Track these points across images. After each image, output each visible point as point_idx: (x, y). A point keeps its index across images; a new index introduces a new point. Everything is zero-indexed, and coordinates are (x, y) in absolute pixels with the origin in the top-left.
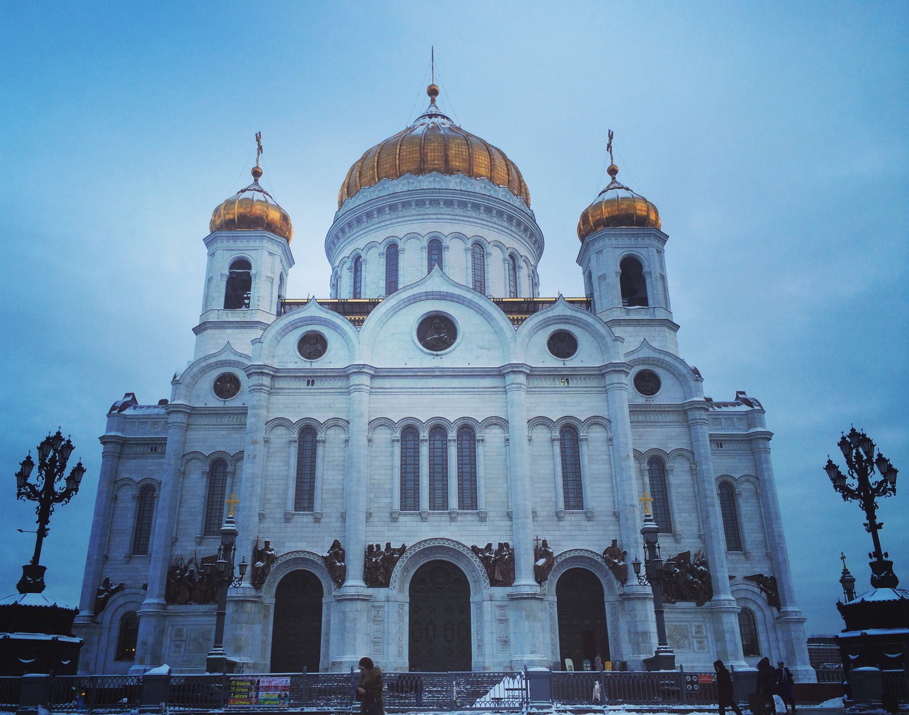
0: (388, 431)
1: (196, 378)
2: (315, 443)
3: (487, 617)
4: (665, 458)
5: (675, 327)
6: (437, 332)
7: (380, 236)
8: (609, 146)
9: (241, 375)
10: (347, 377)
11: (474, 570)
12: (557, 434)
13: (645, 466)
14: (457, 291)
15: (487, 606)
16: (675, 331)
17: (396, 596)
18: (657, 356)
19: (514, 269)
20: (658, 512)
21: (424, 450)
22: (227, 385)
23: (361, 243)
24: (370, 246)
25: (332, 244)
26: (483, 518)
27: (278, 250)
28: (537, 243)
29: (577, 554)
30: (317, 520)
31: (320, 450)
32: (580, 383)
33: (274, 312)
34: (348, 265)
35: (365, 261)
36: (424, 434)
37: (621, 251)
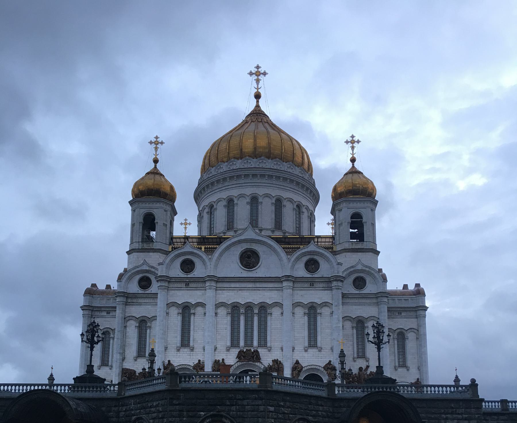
0: (225, 309)
1: (130, 278)
2: (190, 314)
5: (378, 253)
6: (249, 259)
7: (224, 195)
9: (152, 278)
10: (205, 282)
12: (307, 311)
19: (299, 213)
20: (360, 347)
21: (242, 318)
22: (145, 283)
23: (213, 198)
24: (219, 200)
25: (198, 196)
26: (269, 351)
29: (310, 367)
30: (192, 350)
33: (168, 244)
34: (207, 210)
35: (216, 209)
36: (242, 310)
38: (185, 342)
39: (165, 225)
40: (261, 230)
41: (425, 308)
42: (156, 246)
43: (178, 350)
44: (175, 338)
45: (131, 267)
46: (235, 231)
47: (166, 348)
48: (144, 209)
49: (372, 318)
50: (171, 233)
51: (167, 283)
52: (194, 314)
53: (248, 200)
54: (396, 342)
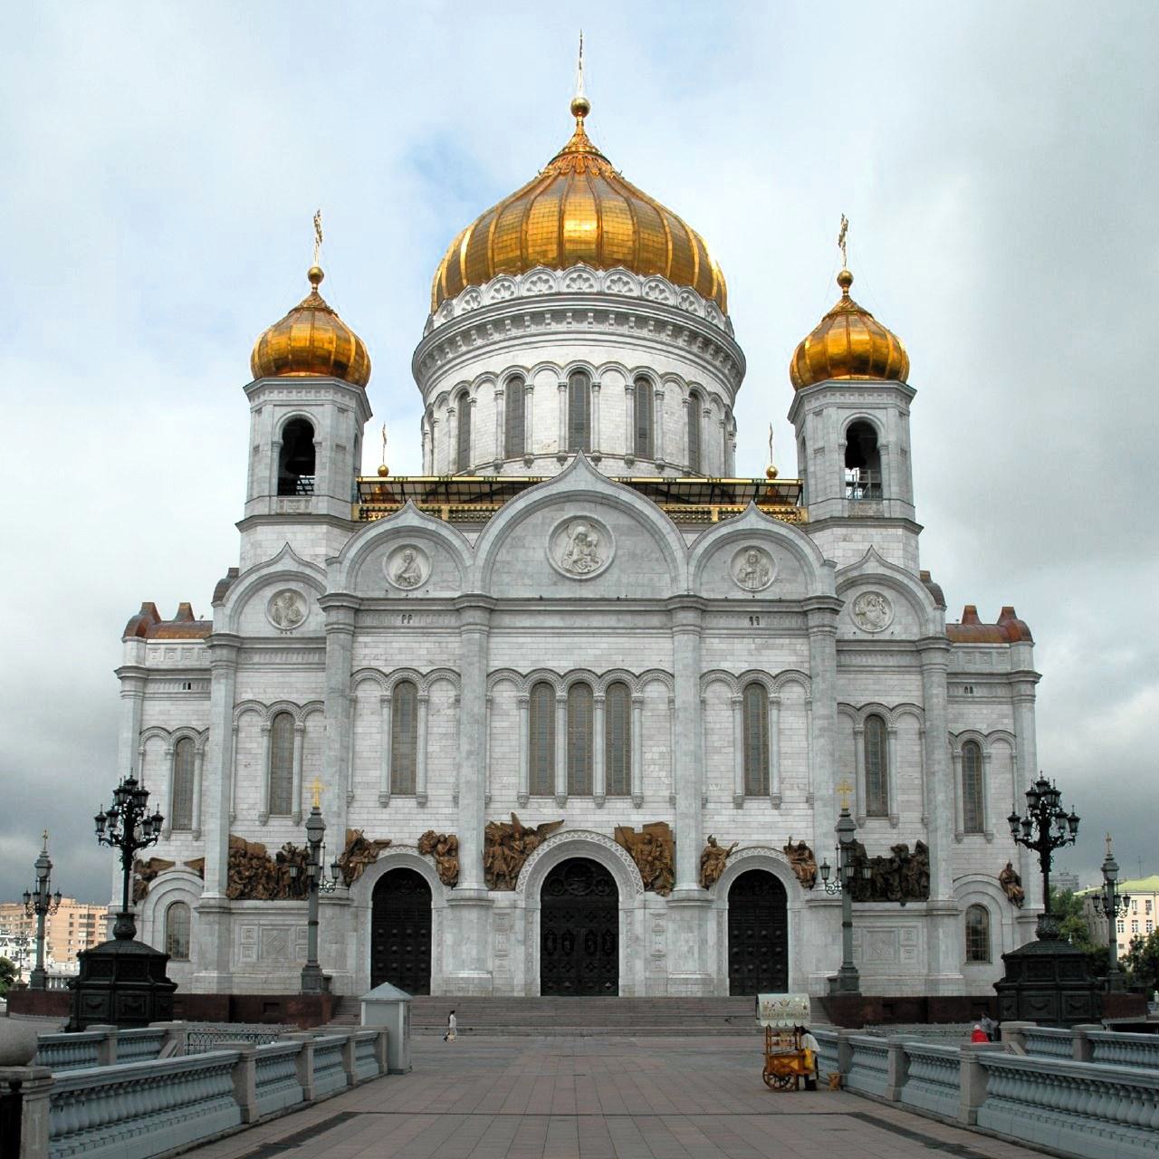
2: (416, 702)
3: (639, 929)
4: (888, 715)
7: (498, 363)
8: (845, 229)
11: (622, 869)
13: (861, 726)
14: (608, 490)
15: (639, 914)
16: (918, 533)
17: (522, 902)
18: (888, 572)
21: (561, 715)
25: (425, 364)
27: (353, 404)
28: (733, 365)
30: (423, 804)
31: (422, 712)
32: (776, 622)
36: (561, 693)
37: (847, 413)
38: (402, 781)
39: (340, 448)
40: (597, 460)
41: (1034, 678)
42: (320, 505)
43: (385, 805)
44: (374, 772)
45: (249, 565)
46: (528, 463)
47: (350, 799)
48: (282, 403)
49: (908, 709)
50: (357, 470)
51: (352, 614)
52: (427, 701)
53: (564, 379)
54: (959, 767)
